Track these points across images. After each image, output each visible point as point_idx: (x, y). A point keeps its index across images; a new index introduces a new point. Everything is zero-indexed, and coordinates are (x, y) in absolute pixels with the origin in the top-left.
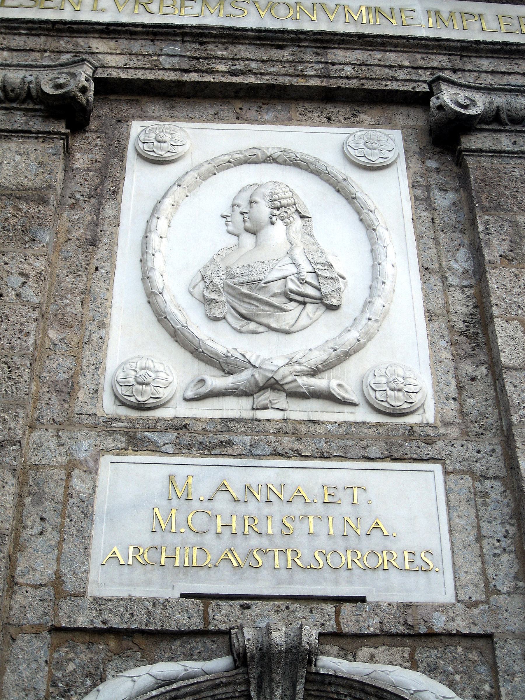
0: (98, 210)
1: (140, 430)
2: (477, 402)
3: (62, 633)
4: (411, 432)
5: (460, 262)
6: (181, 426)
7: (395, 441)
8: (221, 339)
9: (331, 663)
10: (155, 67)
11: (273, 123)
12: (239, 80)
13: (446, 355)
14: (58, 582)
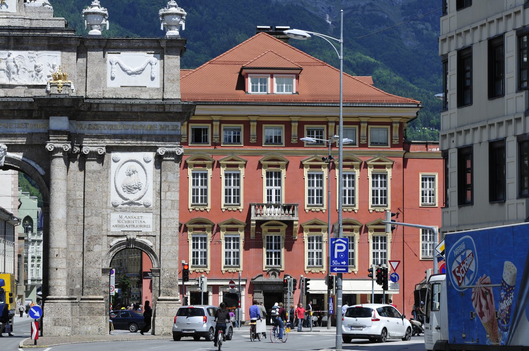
0: (108, 171)
2: (158, 204)
3: (108, 236)
8: (125, 195)
9: (138, 239)
12: (128, 145)
13: (155, 196)
14: (107, 230)
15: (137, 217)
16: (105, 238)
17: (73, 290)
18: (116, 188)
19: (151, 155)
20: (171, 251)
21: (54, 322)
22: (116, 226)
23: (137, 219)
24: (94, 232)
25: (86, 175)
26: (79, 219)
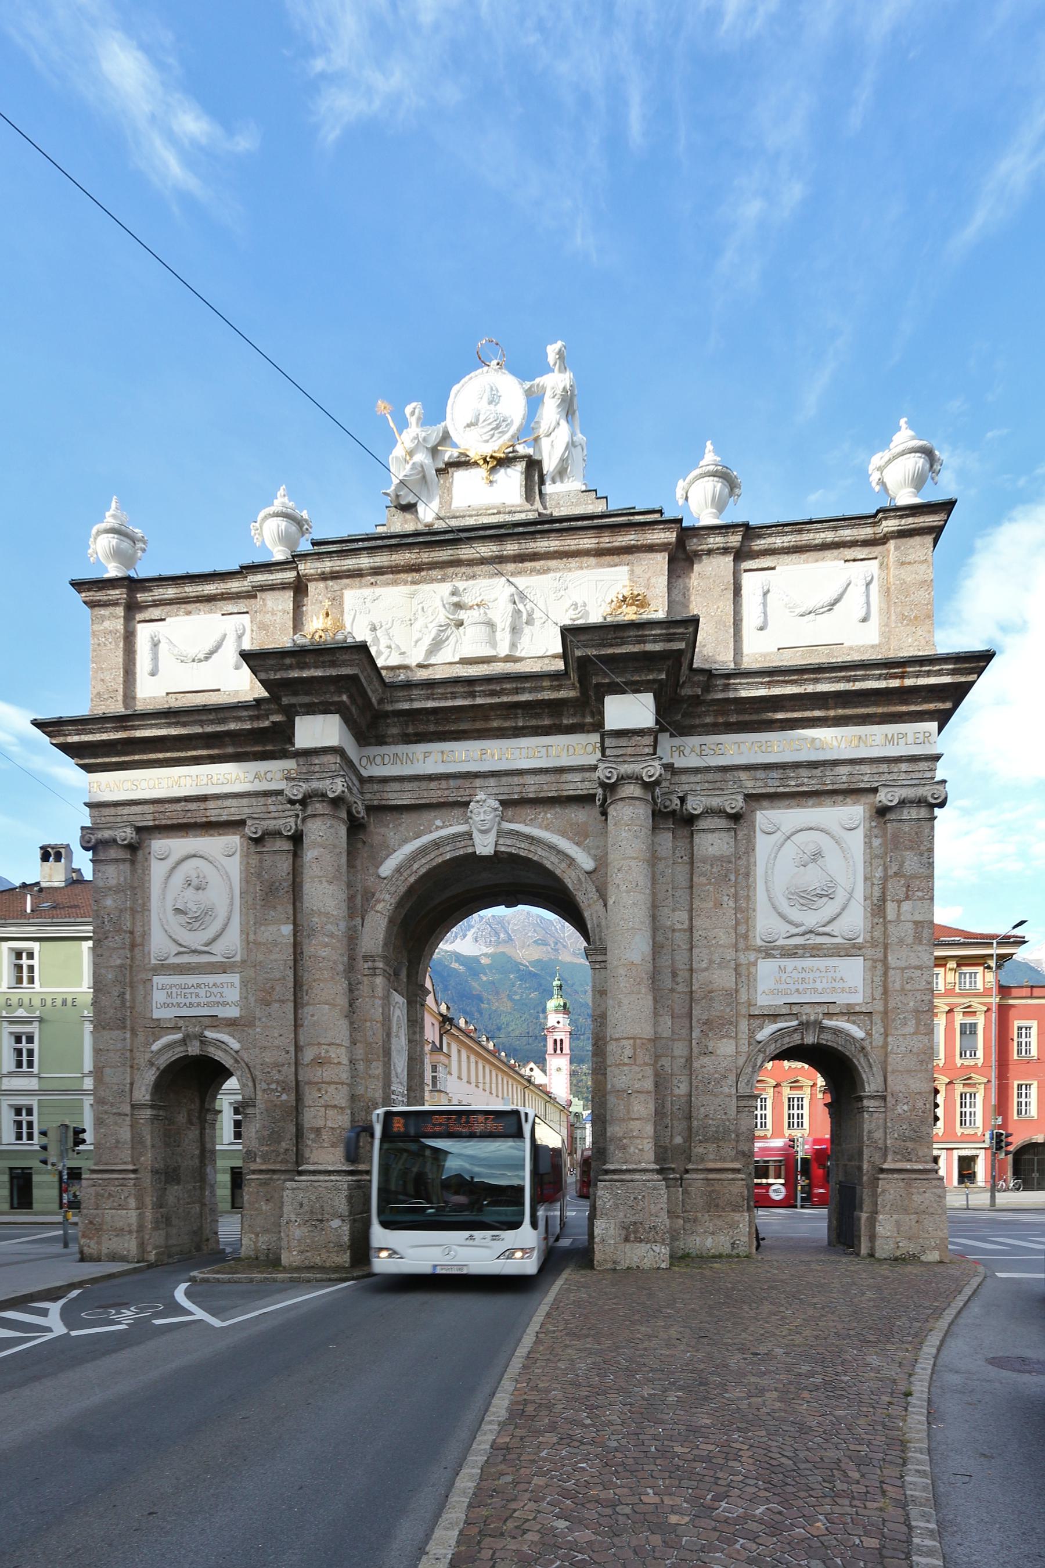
1: (768, 951)
4: (854, 946)
5: (879, 873)
6: (782, 948)
7: (849, 949)
8: (795, 914)
9: (827, 1022)
10: (766, 786)
11: (812, 807)
15: (823, 969)
16: (744, 1025)
17: (665, 1148)
18: (770, 899)
19: (855, 812)
20: (915, 1050)
21: (624, 1232)
22: (772, 992)
23: (823, 974)
24: (719, 1007)
25: (696, 870)
26: (679, 979)
